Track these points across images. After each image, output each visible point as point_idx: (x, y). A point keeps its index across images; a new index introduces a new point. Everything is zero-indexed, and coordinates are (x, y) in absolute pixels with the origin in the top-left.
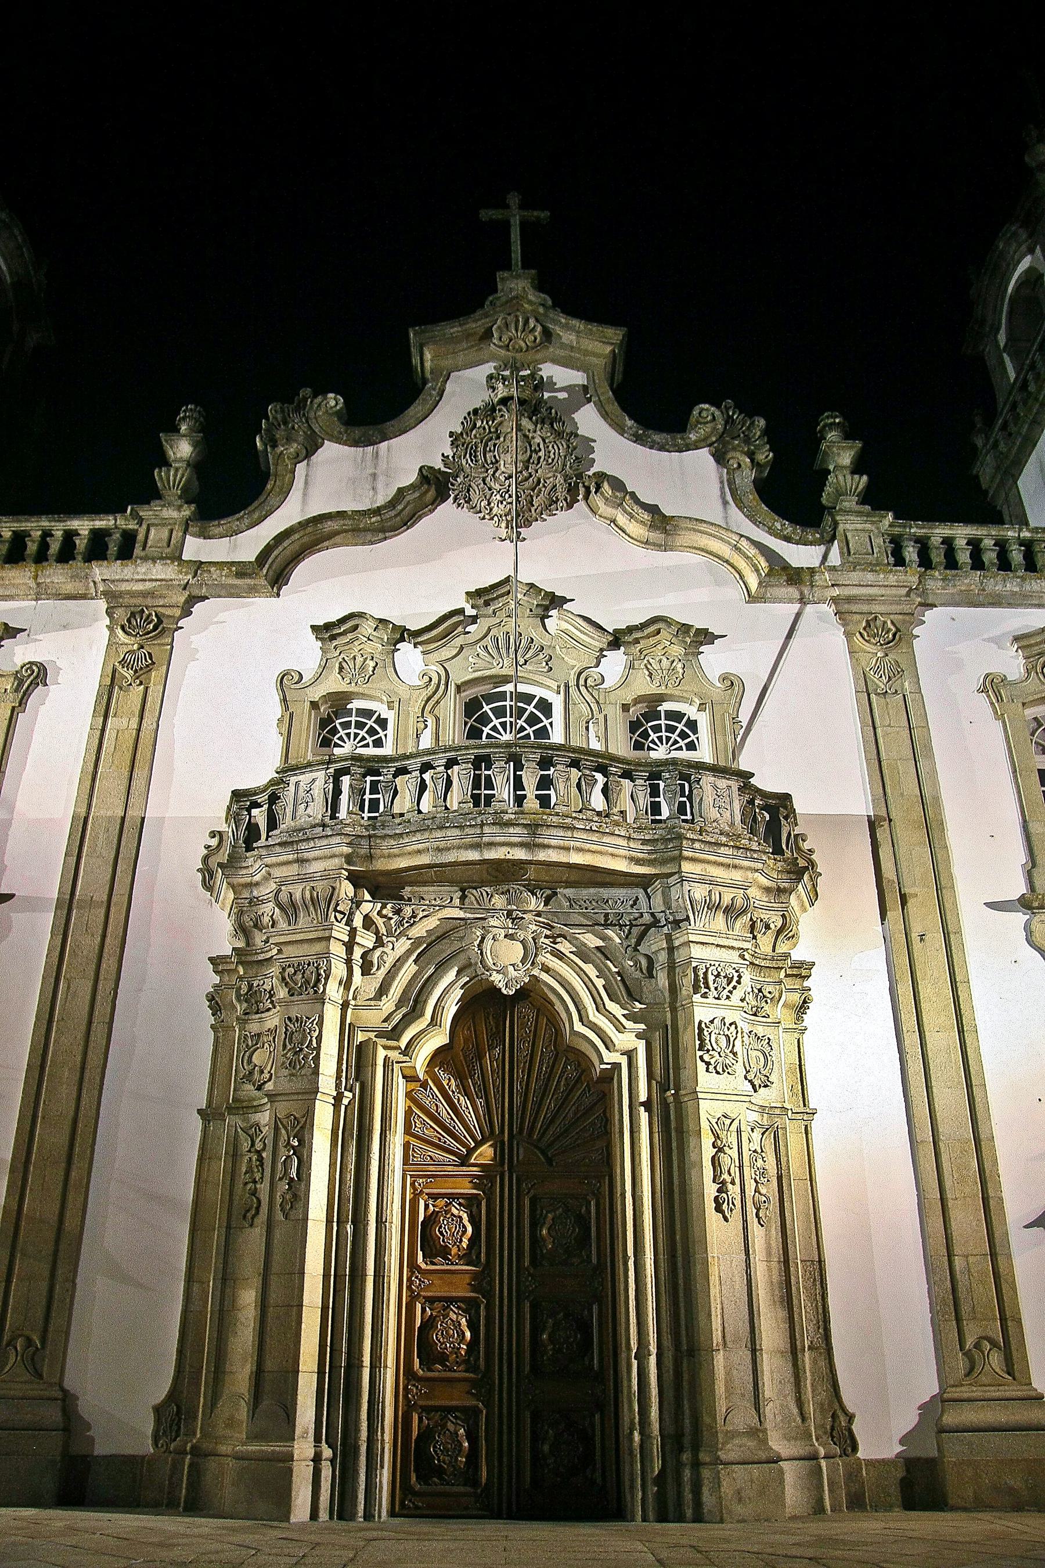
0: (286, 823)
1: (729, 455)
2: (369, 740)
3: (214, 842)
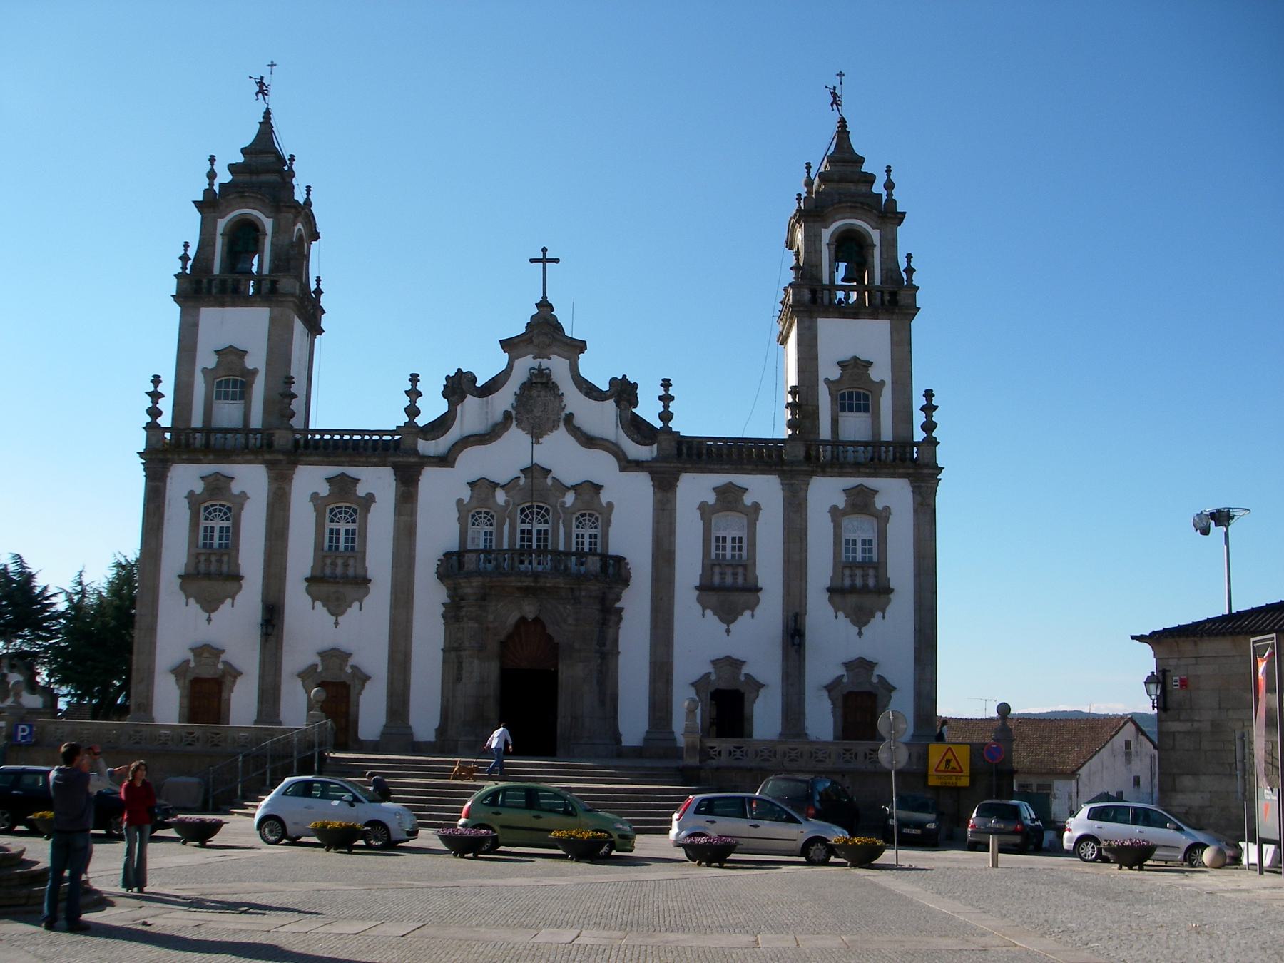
0: (465, 569)
1: (622, 402)
2: (488, 523)
3: (439, 563)
